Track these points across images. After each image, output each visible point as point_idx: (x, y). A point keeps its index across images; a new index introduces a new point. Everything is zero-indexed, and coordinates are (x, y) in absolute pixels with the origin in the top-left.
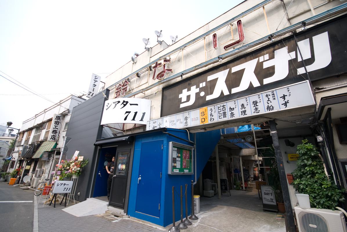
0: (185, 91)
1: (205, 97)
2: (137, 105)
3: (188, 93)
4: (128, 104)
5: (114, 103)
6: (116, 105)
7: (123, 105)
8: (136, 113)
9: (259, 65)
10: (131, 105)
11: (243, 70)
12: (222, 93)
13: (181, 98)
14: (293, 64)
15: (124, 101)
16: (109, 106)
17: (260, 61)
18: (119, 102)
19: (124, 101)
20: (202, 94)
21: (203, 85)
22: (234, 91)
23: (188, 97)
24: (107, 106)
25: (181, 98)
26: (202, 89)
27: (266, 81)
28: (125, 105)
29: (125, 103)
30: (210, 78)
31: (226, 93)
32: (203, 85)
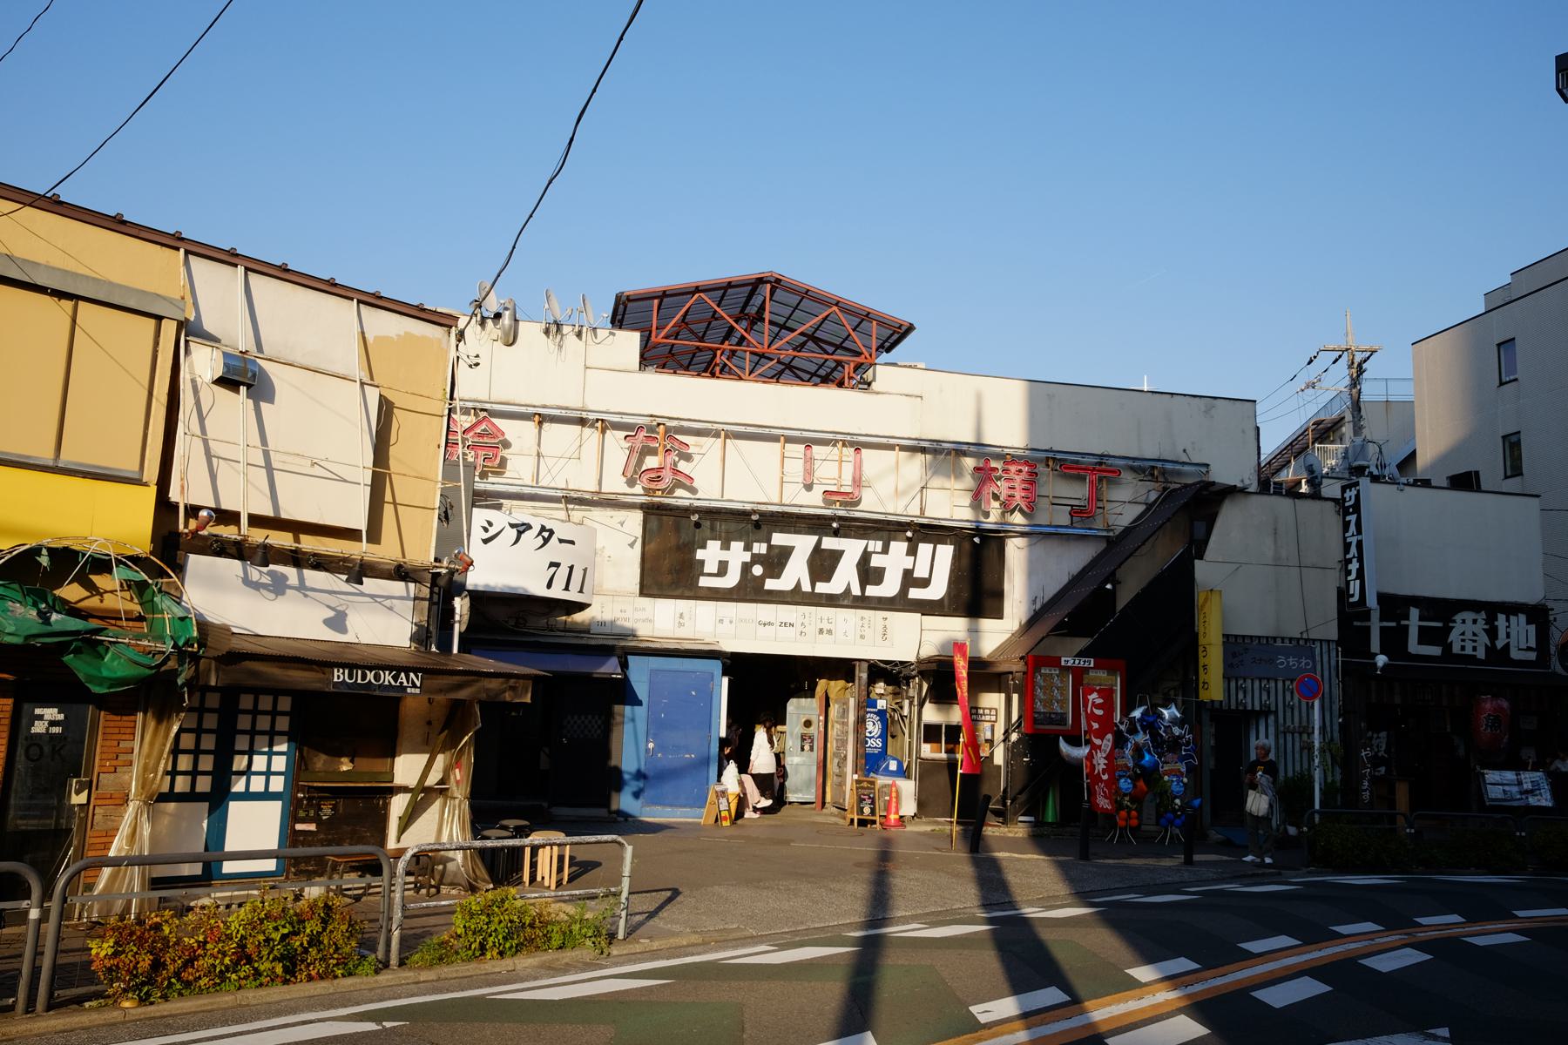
0: (714, 546)
1: (762, 579)
2: (572, 542)
3: (724, 556)
4: (554, 539)
5: (512, 526)
6: (520, 533)
7: (540, 541)
8: (571, 568)
9: (866, 556)
10: (561, 541)
11: (841, 553)
12: (798, 585)
13: (702, 562)
14: (909, 579)
15: (543, 529)
16: (492, 531)
17: (870, 549)
18: (529, 527)
19: (543, 529)
20: (758, 570)
21: (760, 548)
22: (822, 588)
23: (723, 569)
24: (486, 530)
25: (702, 562)
26: (756, 559)
27: (872, 591)
28: (546, 541)
29: (546, 534)
30: (778, 539)
31: (806, 587)
32: (760, 548)
